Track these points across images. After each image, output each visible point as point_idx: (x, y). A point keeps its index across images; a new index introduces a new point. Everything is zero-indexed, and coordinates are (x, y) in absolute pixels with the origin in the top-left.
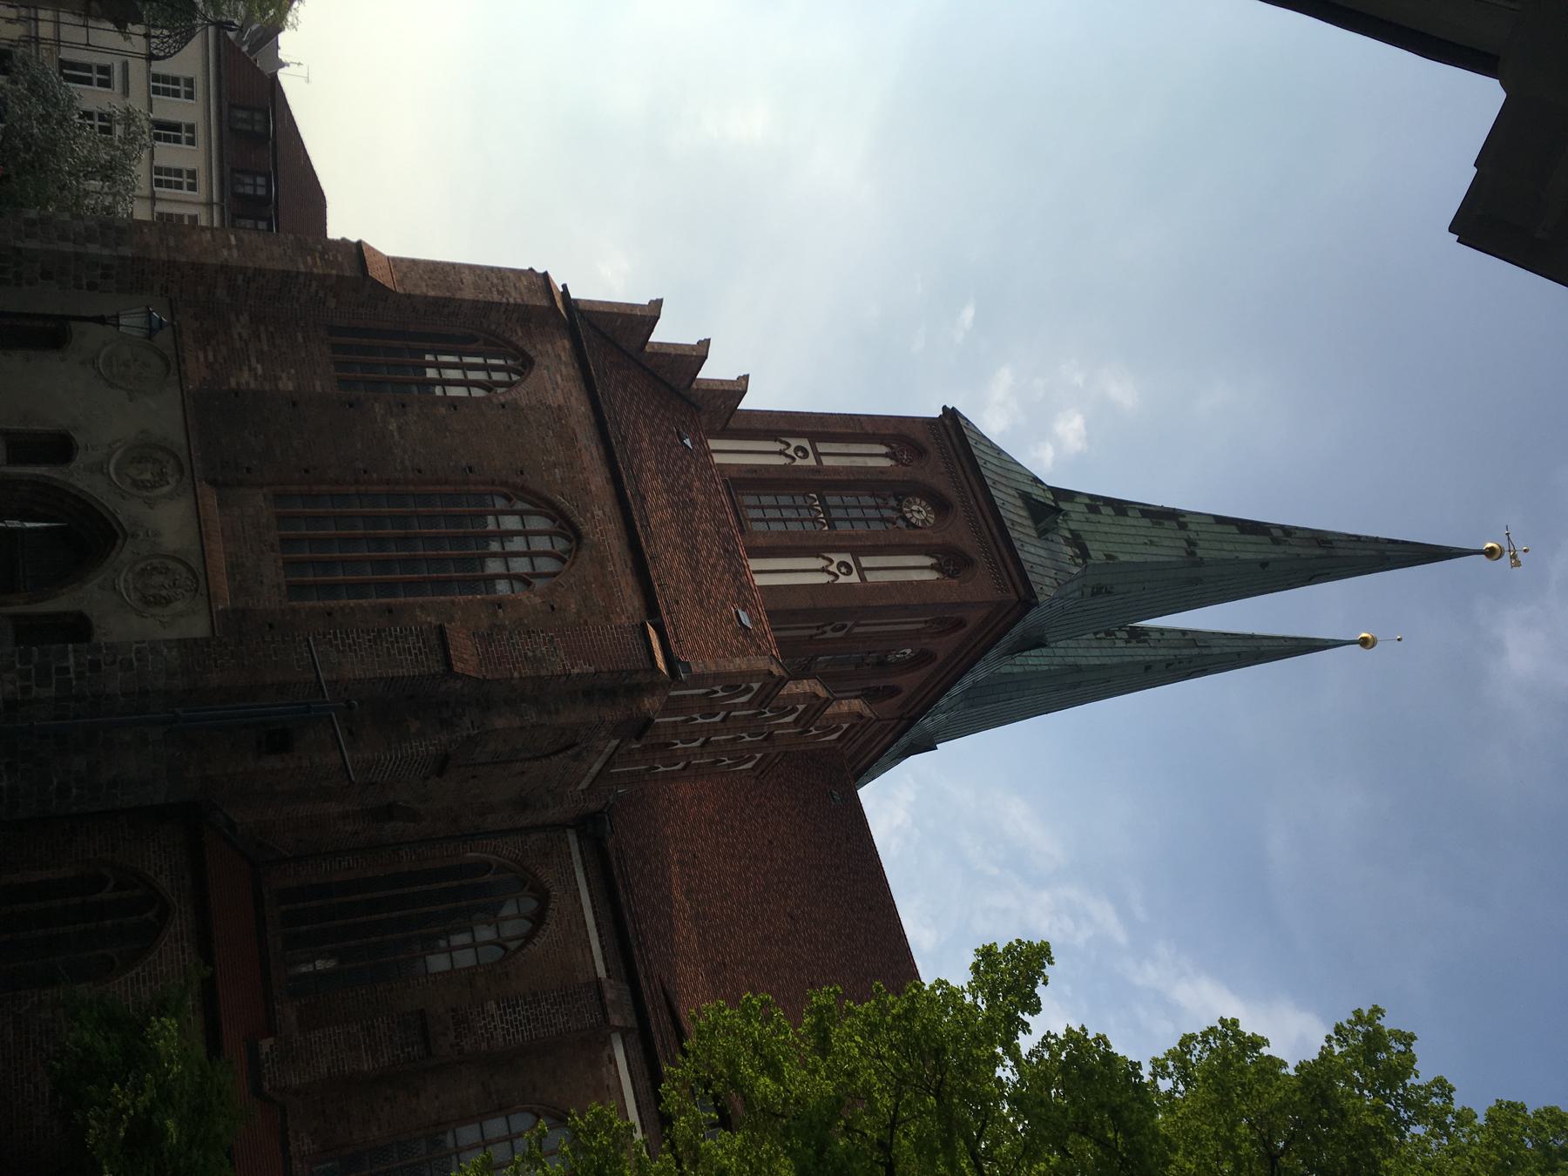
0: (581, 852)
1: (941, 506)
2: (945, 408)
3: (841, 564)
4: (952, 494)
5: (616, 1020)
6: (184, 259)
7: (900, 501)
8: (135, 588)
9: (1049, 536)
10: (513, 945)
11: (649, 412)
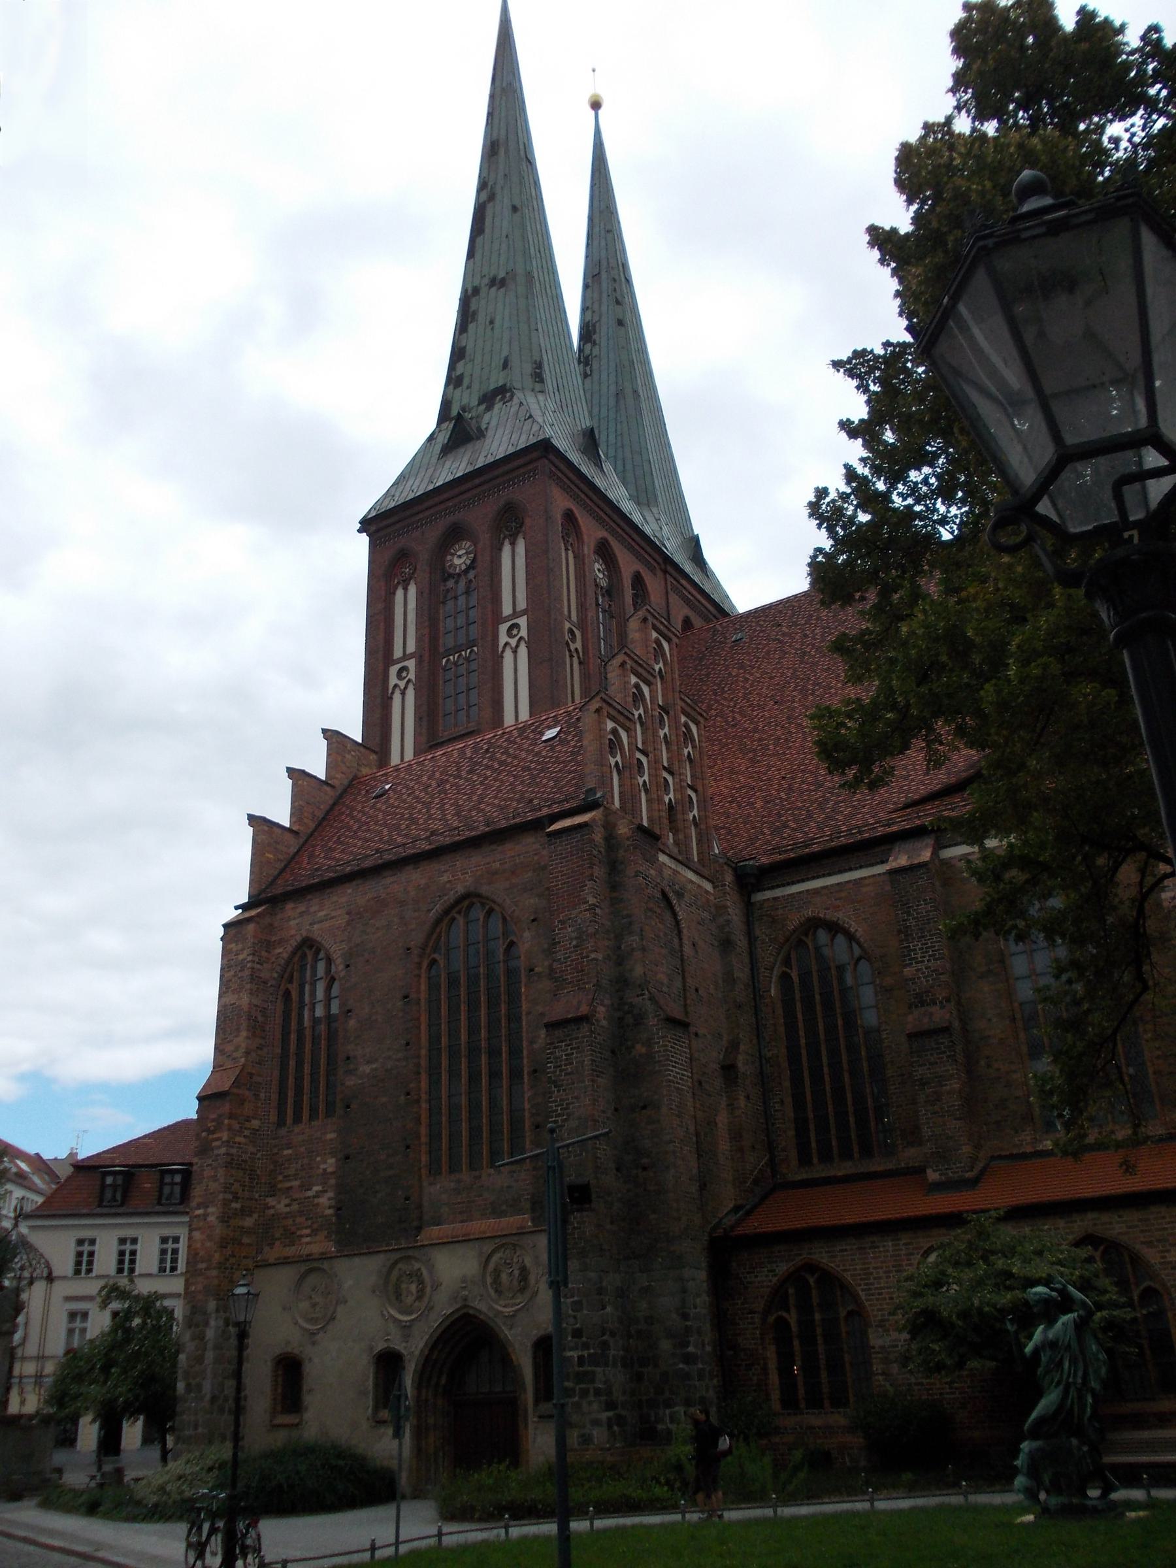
0: (773, 888)
1: (455, 534)
2: (359, 531)
3: (510, 635)
4: (442, 524)
5: (926, 855)
6: (217, 1256)
7: (451, 576)
8: (513, 1298)
9: (484, 427)
10: (857, 951)
11: (355, 827)
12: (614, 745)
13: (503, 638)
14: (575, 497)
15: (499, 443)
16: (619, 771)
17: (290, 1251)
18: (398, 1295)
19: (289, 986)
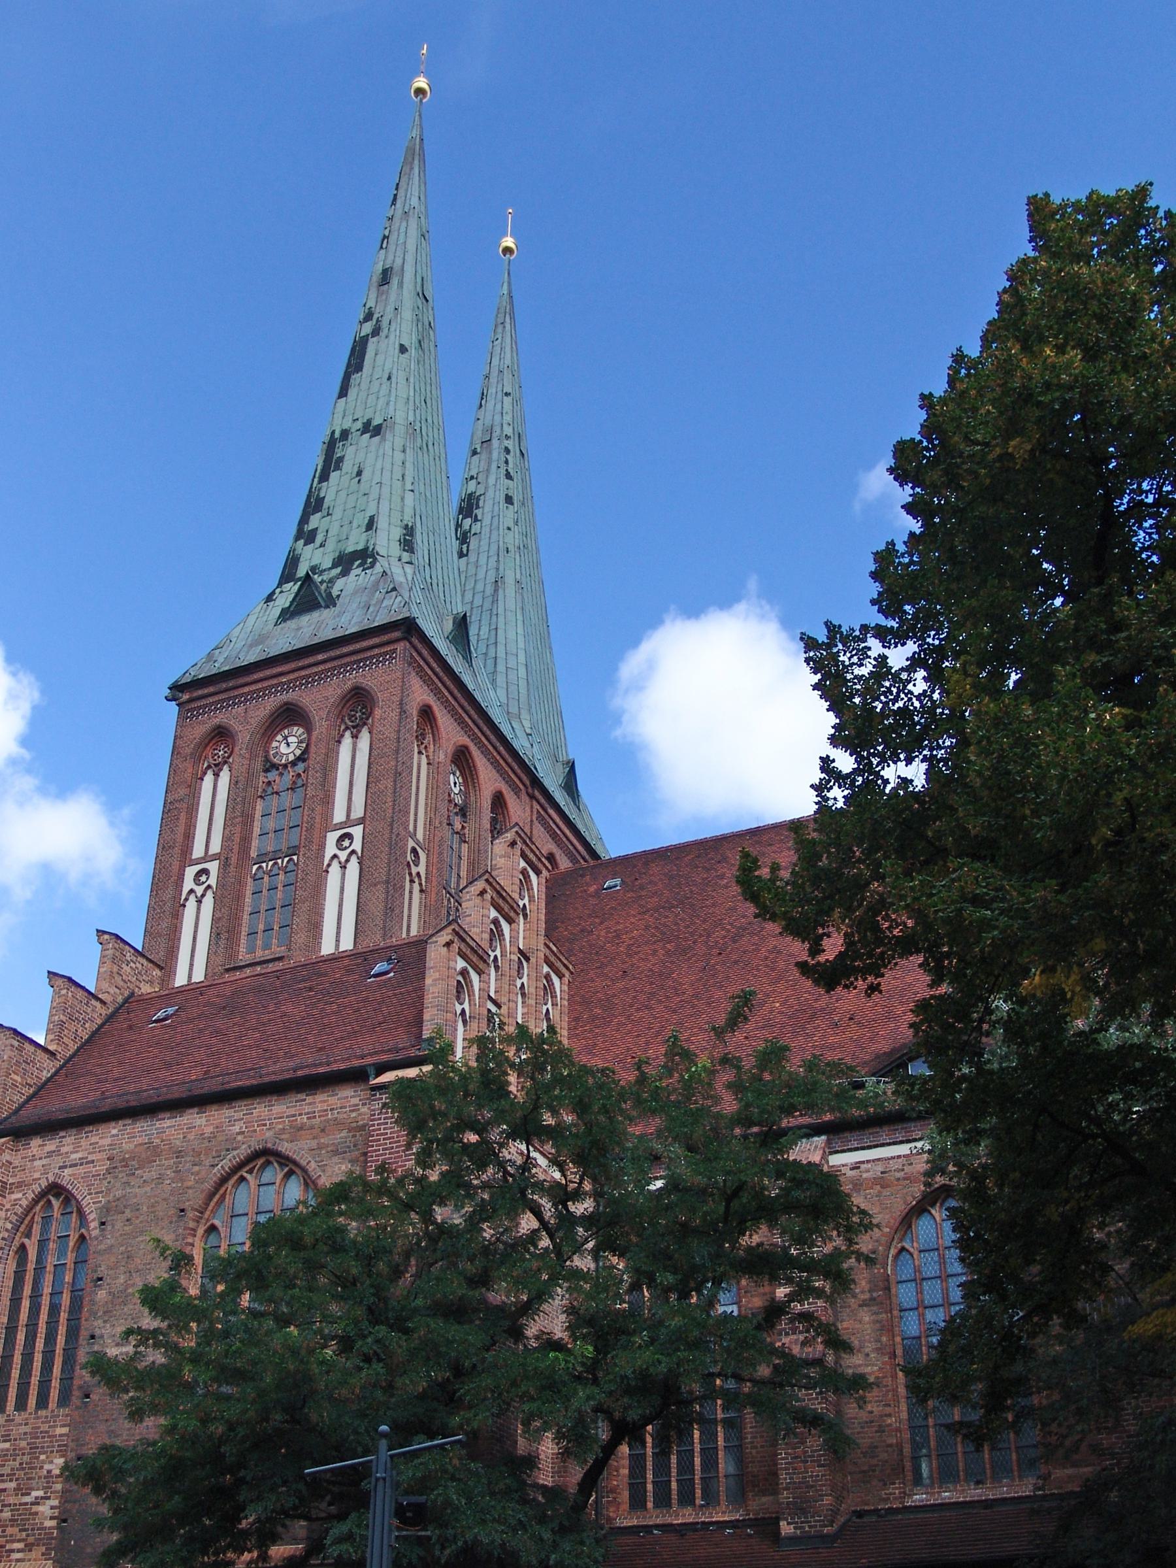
4: (271, 703)
7: (275, 766)
9: (335, 592)
13: (331, 849)
14: (436, 692)
16: (465, 1022)
19: (26, 1241)
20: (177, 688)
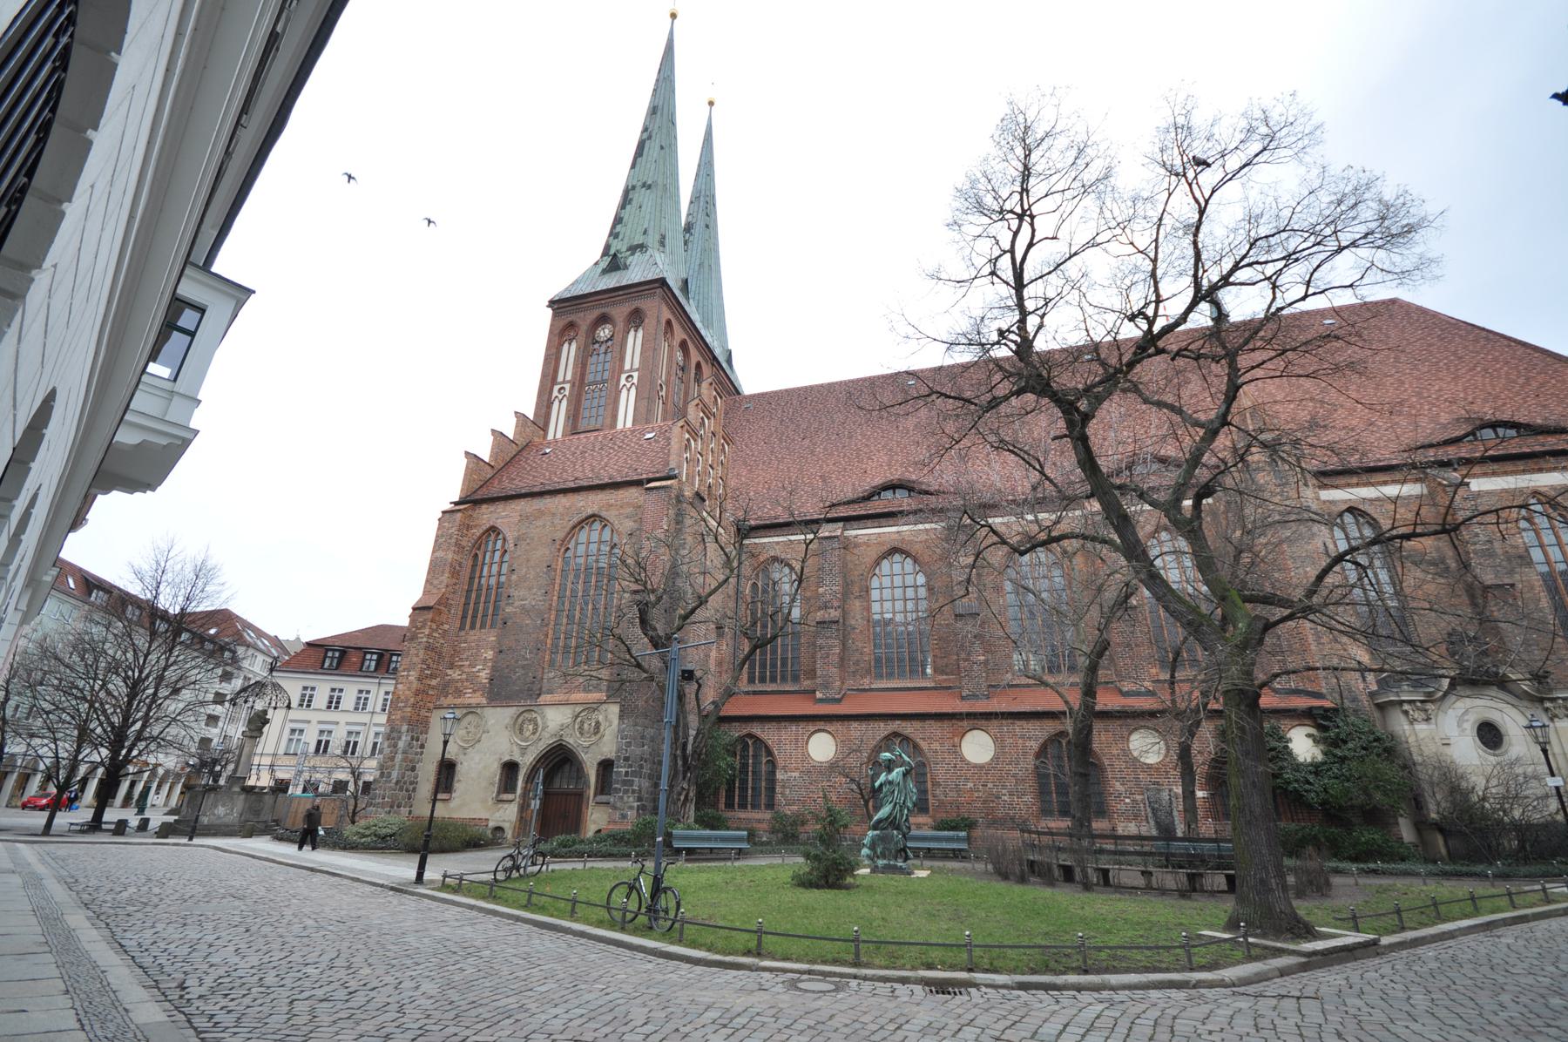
1: (604, 319)
4: (596, 313)
5: (838, 533)
12: (687, 447)
15: (637, 271)
17: (458, 701)
18: (521, 731)
20: (552, 303)
